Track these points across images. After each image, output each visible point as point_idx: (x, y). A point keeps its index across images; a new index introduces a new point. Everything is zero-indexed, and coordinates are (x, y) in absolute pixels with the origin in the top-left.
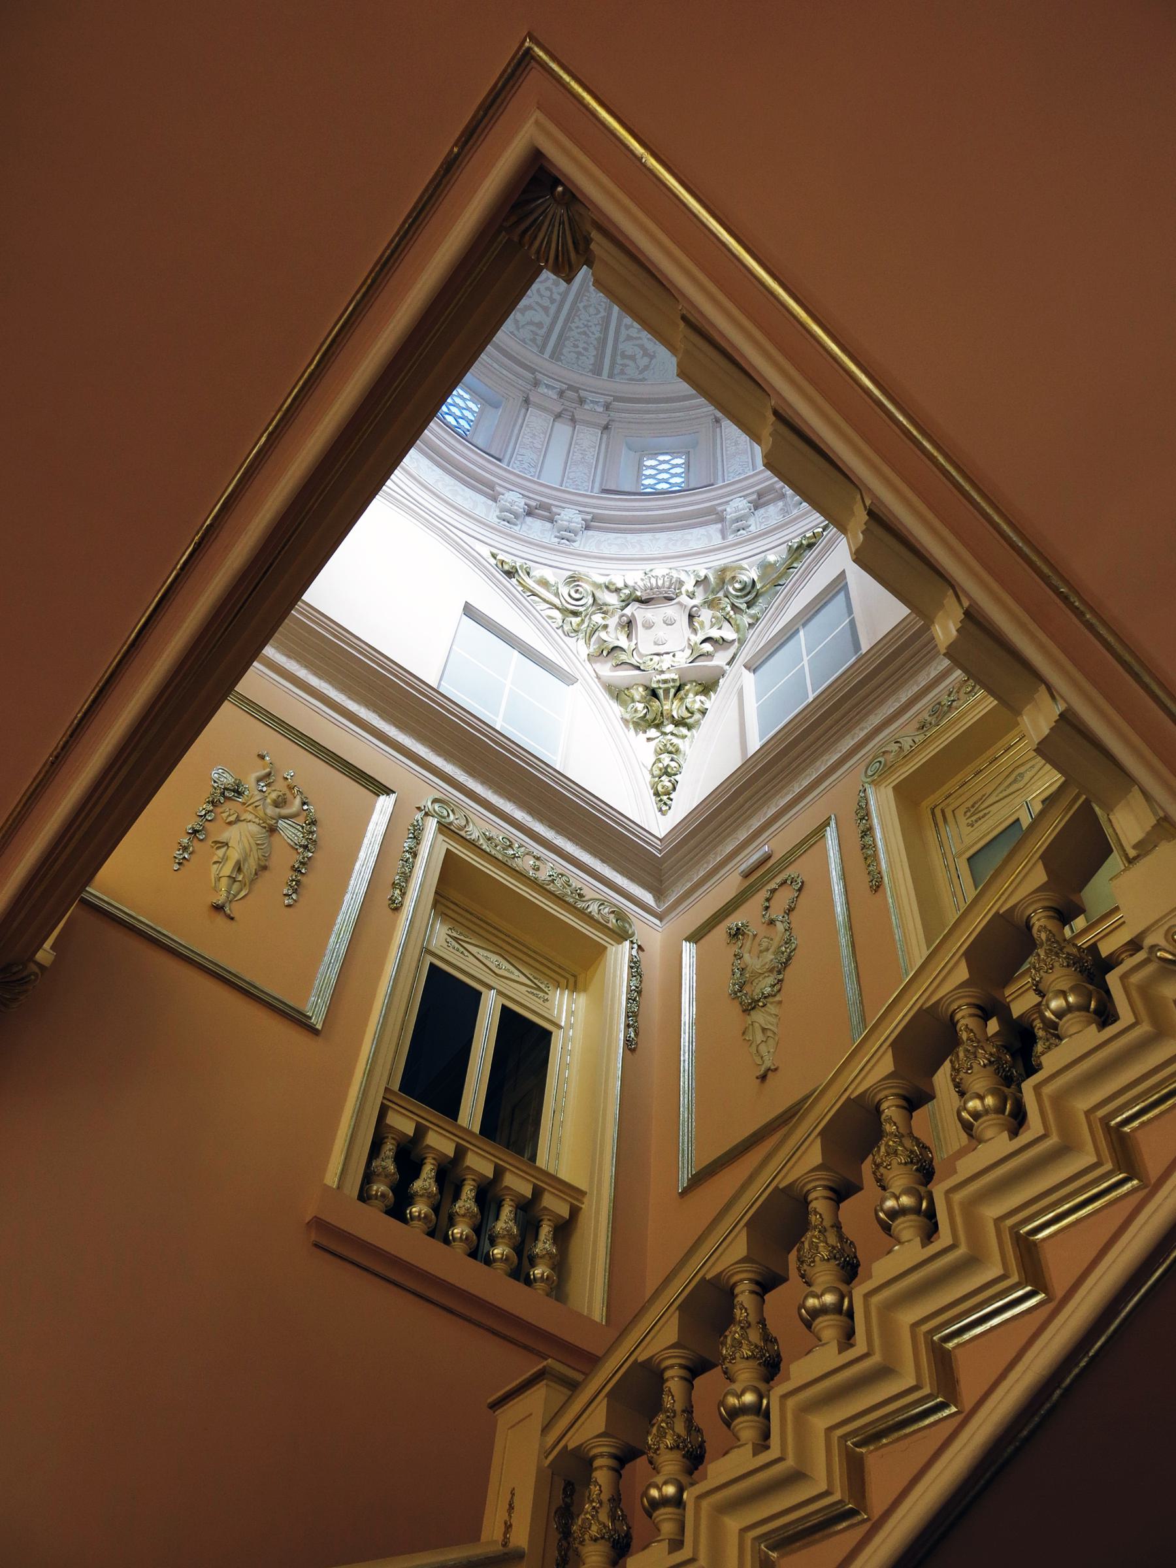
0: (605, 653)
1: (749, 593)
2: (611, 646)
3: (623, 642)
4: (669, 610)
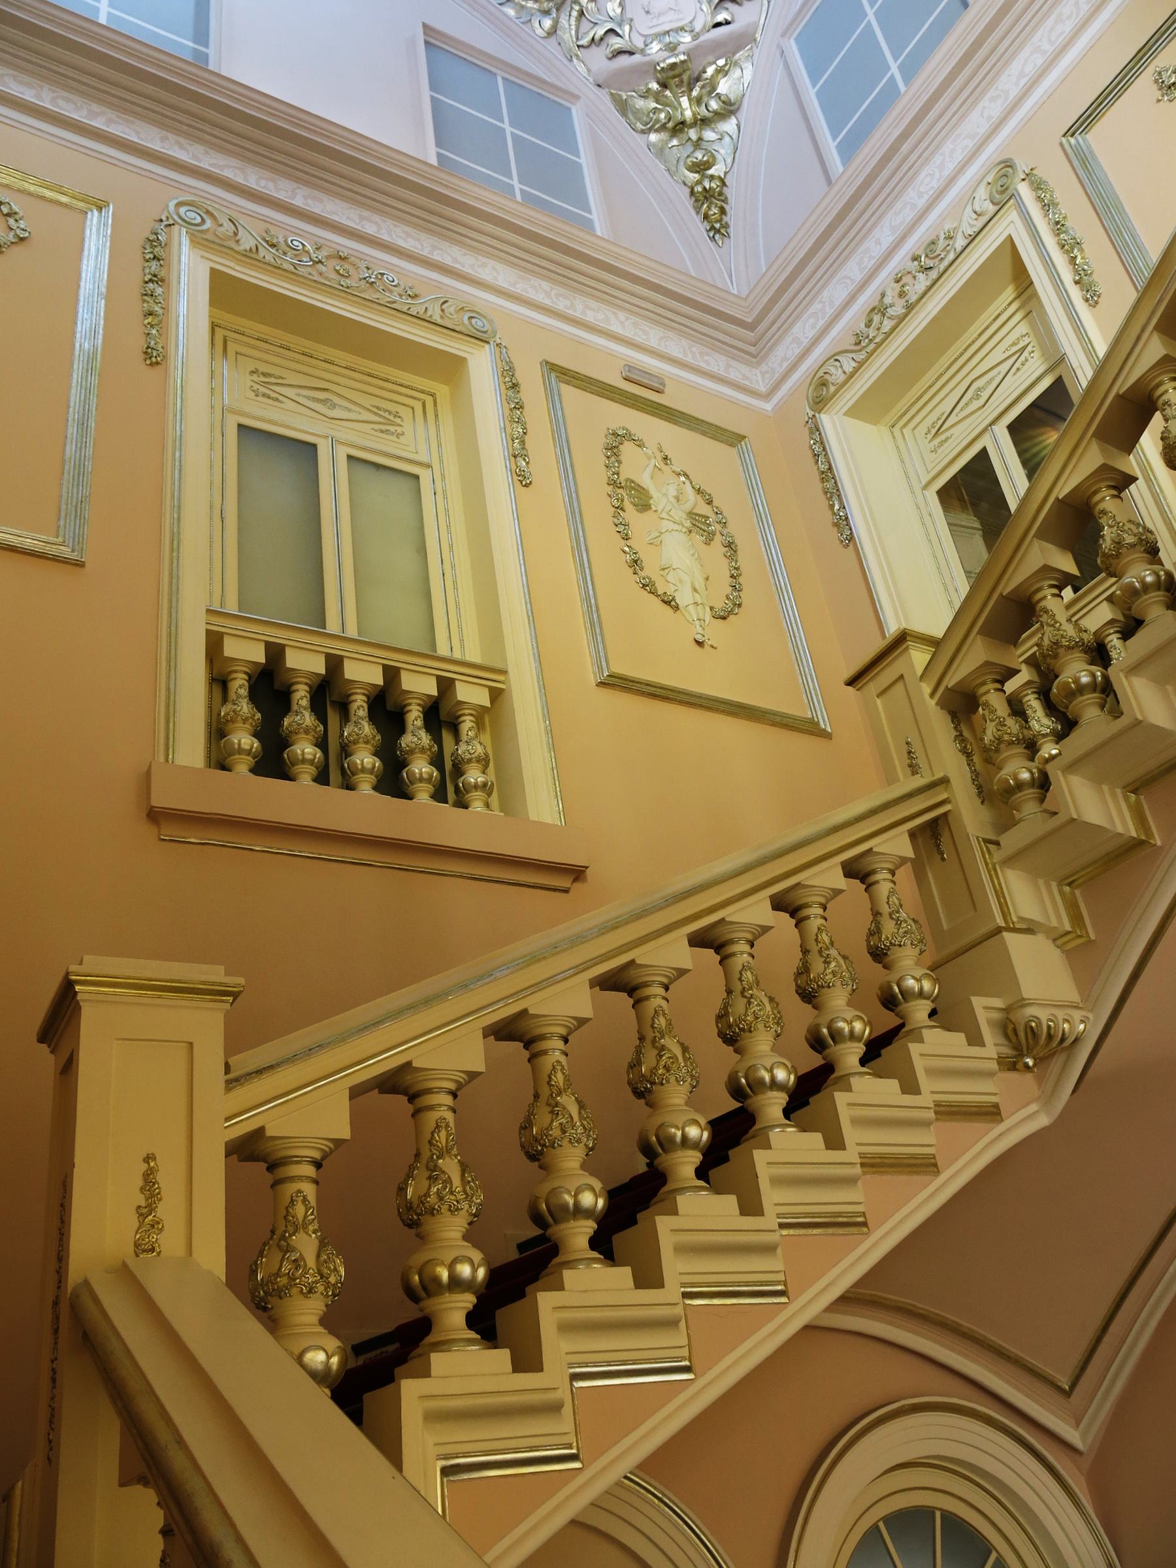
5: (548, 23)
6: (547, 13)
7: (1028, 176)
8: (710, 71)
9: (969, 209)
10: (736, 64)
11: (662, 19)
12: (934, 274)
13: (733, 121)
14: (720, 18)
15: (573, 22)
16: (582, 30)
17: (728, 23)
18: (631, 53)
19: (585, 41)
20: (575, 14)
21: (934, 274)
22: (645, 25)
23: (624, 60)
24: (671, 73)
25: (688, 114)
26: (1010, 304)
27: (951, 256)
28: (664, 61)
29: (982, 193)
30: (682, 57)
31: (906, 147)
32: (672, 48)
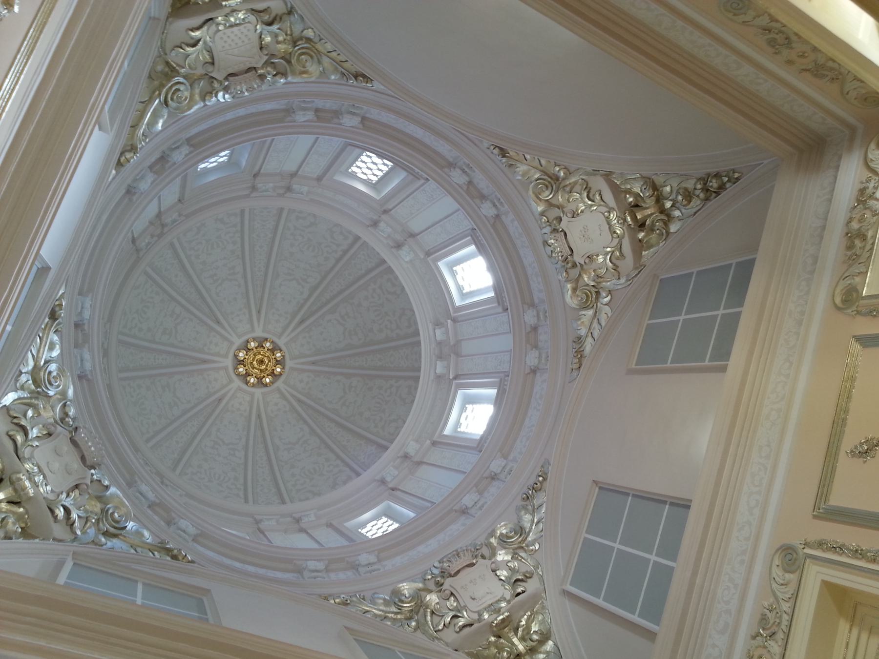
0: (16, 421)
1: (115, 528)
2: (23, 422)
3: (34, 433)
4: (76, 464)
5: (414, 624)
6: (410, 618)
7: (806, 544)
8: (523, 622)
9: (774, 585)
10: (537, 613)
11: (483, 600)
12: (780, 635)
13: (550, 643)
14: (519, 590)
15: (429, 618)
16: (435, 622)
17: (523, 592)
18: (471, 625)
19: (440, 627)
20: (429, 614)
21: (780, 635)
22: (473, 606)
23: (467, 630)
24: (502, 626)
25: (521, 647)
26: (850, 631)
27: (786, 617)
28: (496, 619)
29: (777, 572)
30: (506, 614)
31: (698, 581)
32: (498, 611)
